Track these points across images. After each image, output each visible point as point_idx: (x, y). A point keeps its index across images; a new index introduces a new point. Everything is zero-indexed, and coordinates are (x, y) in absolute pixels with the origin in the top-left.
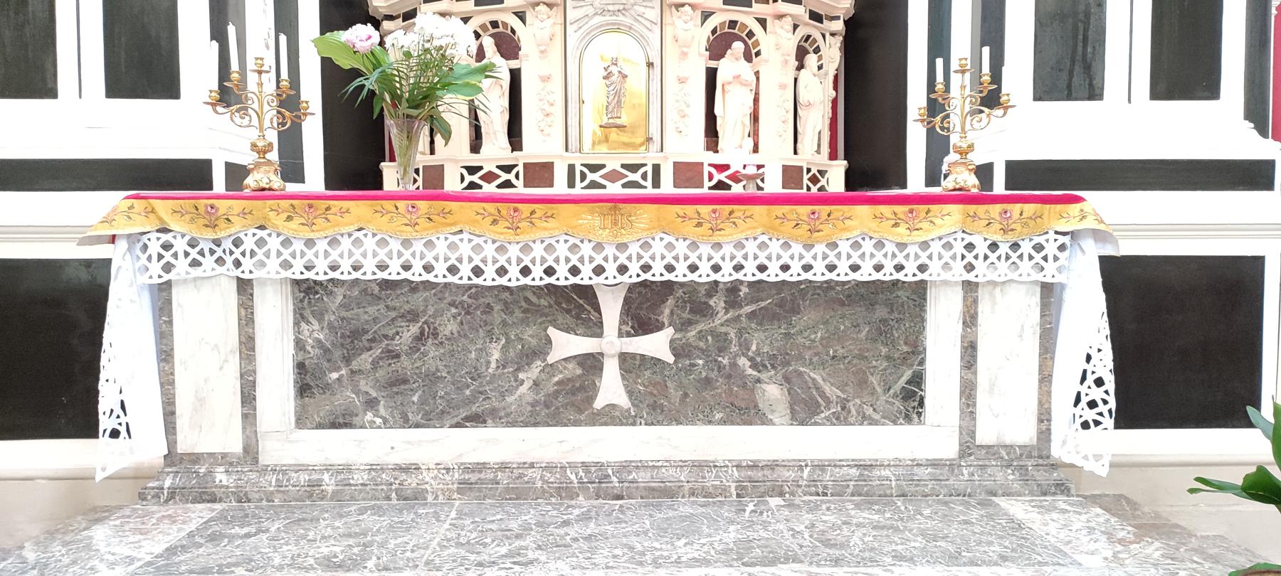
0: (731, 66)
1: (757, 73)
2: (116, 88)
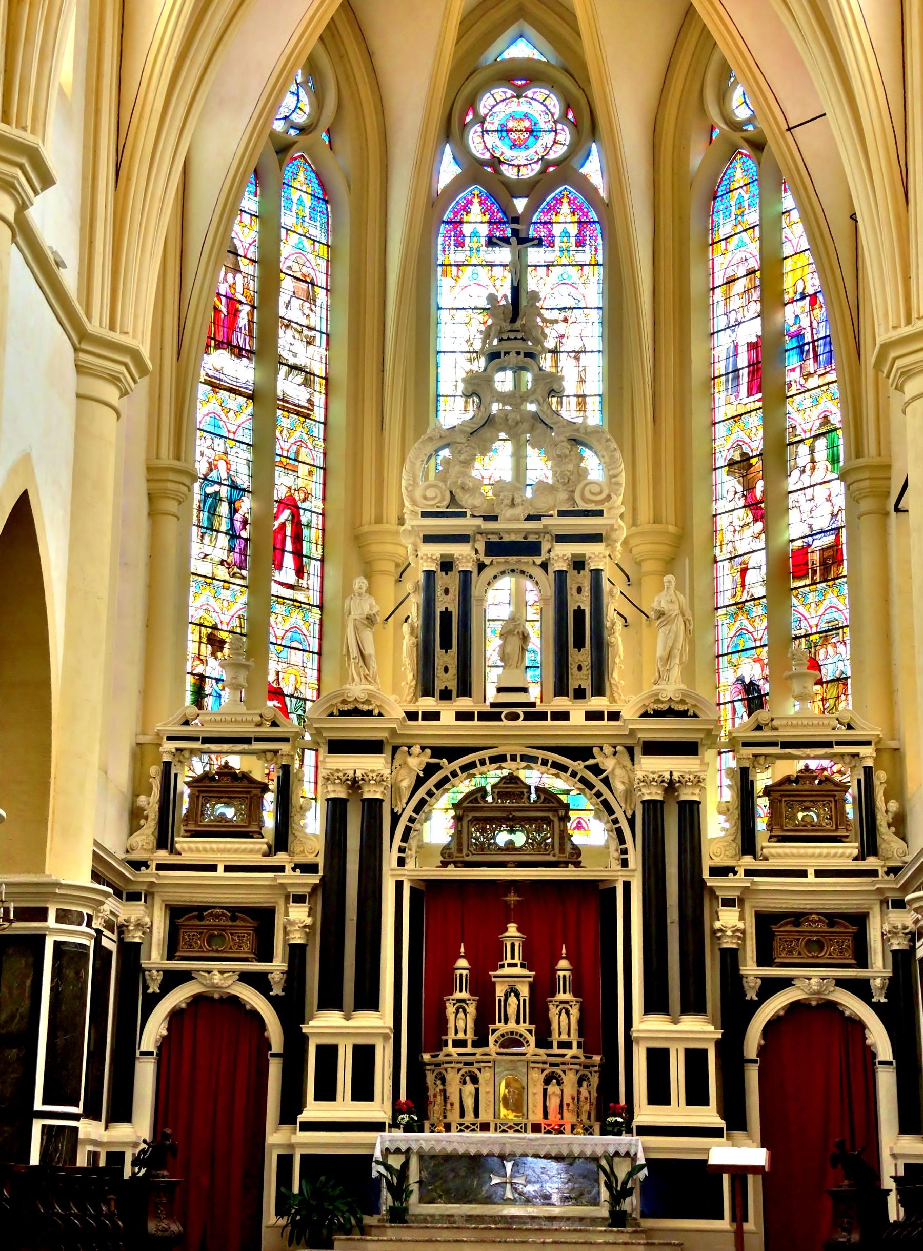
0: (553, 1089)
1: (562, 1091)
2: (355, 1098)
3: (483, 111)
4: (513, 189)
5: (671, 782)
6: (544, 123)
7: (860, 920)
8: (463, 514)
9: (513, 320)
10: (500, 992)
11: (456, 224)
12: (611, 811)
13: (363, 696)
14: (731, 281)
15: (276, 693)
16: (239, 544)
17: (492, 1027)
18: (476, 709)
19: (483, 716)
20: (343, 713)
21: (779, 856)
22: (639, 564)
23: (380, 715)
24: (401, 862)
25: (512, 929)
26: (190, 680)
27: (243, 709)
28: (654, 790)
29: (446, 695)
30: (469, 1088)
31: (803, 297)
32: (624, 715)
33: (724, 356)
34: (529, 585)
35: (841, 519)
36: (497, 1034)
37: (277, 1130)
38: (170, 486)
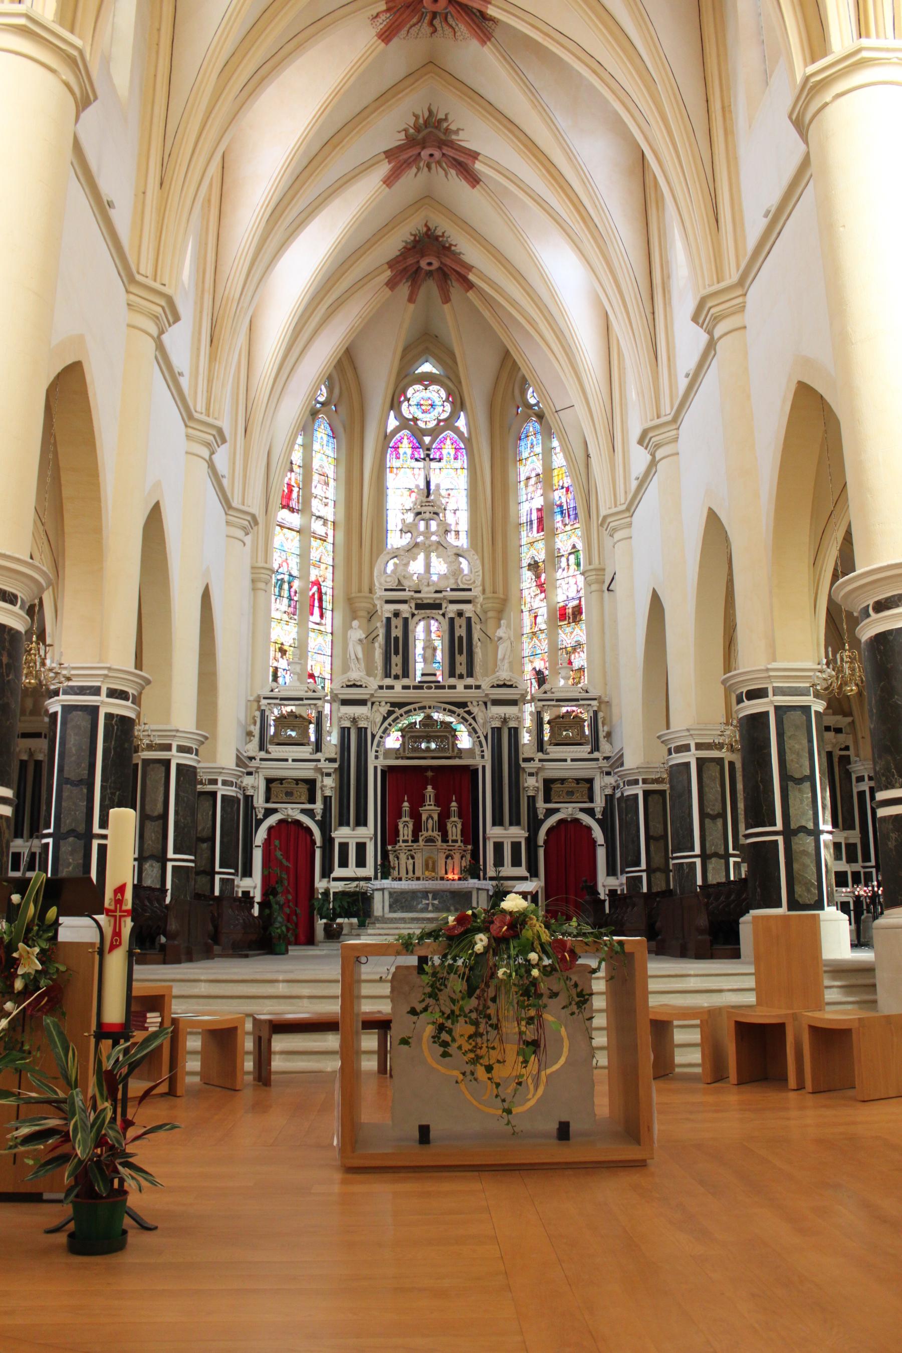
0: (449, 861)
3: (409, 395)
4: (425, 432)
5: (505, 719)
6: (438, 402)
7: (590, 781)
8: (404, 590)
9: (428, 496)
10: (424, 817)
11: (396, 448)
12: (476, 732)
13: (358, 678)
14: (528, 478)
15: (312, 676)
16: (293, 603)
17: (420, 834)
18: (412, 684)
19: (415, 688)
20: (348, 686)
21: (555, 752)
22: (485, 612)
23: (366, 687)
24: (377, 757)
25: (430, 788)
26: (271, 670)
27: (298, 684)
28: (497, 722)
29: (397, 677)
30: (411, 861)
31: (562, 488)
32: (483, 687)
33: (525, 514)
34: (432, 622)
35: (582, 593)
36: (423, 837)
37: (320, 881)
38: (262, 576)
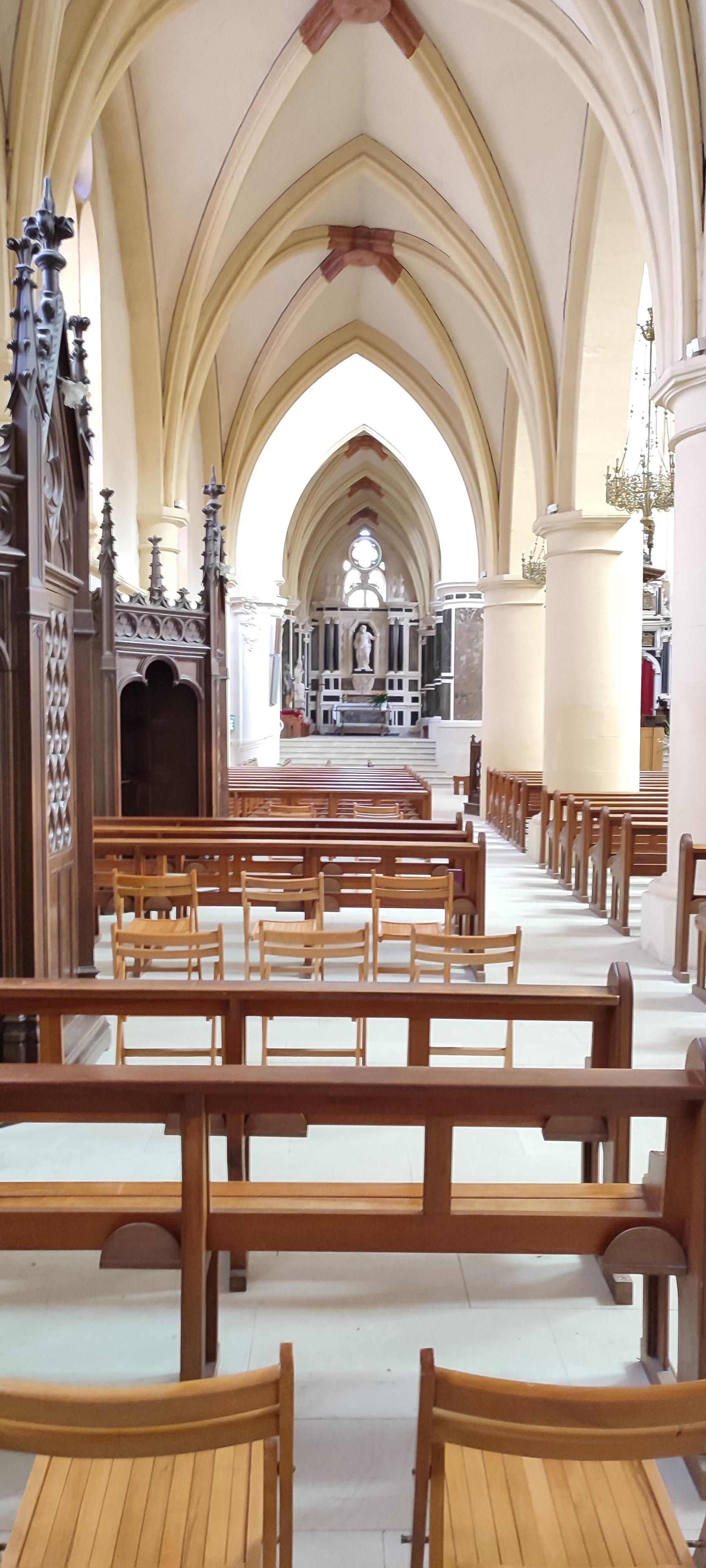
7: (653, 633)
